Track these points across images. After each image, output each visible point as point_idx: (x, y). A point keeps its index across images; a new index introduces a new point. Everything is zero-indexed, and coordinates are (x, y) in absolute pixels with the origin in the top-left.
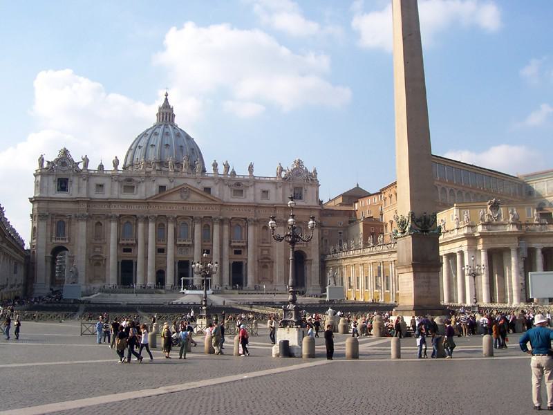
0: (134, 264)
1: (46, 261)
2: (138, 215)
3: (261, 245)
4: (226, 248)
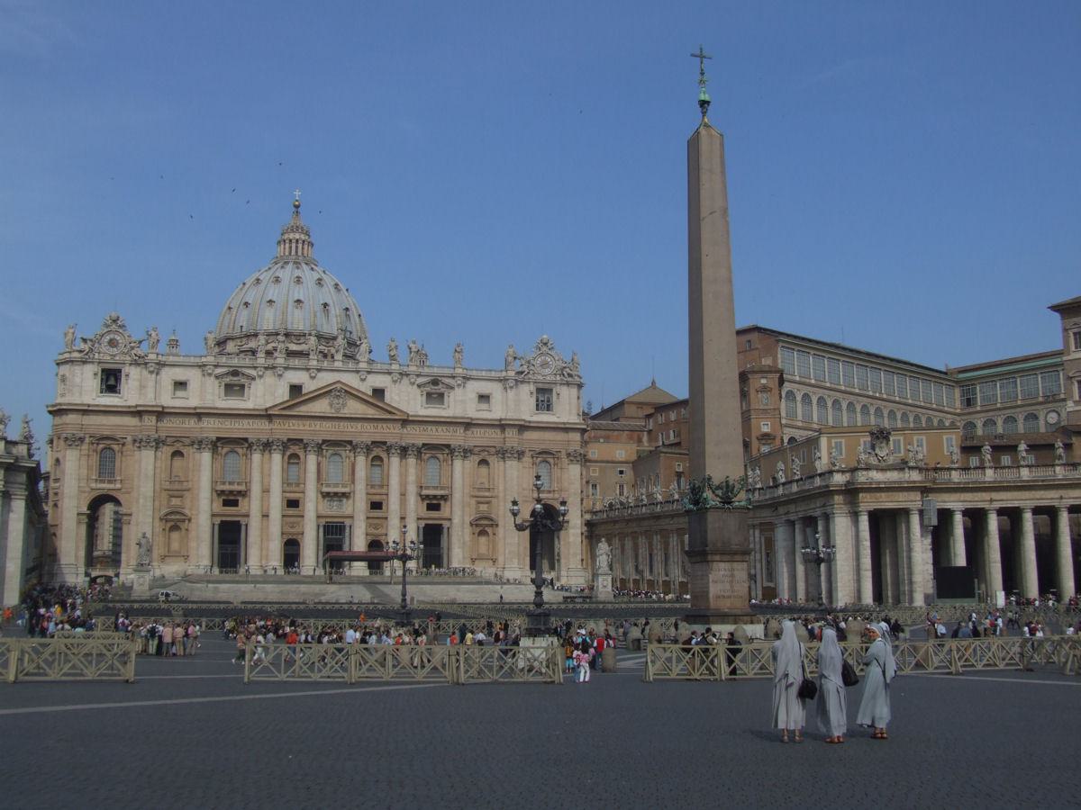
0: (243, 528)
1: (79, 522)
2: (252, 437)
3: (477, 494)
4: (412, 499)
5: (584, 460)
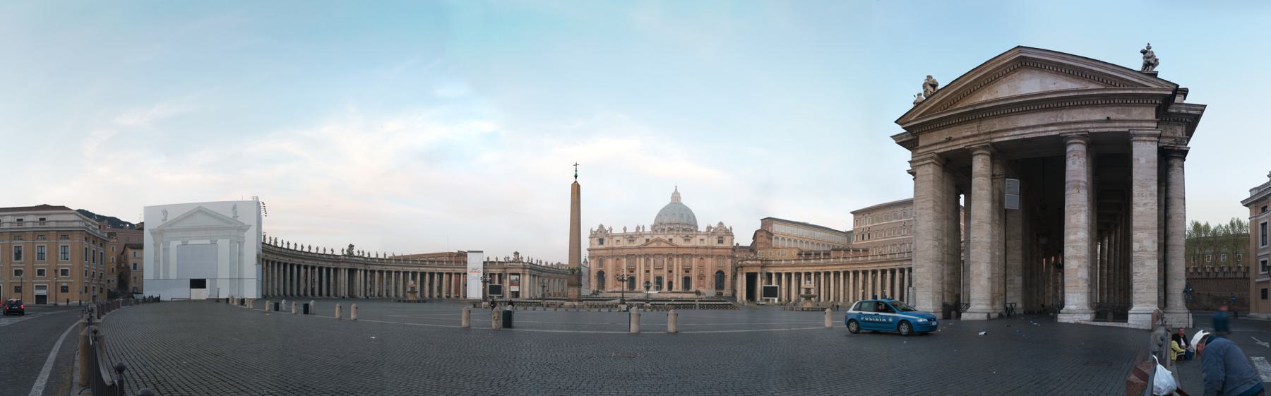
5: (733, 257)
